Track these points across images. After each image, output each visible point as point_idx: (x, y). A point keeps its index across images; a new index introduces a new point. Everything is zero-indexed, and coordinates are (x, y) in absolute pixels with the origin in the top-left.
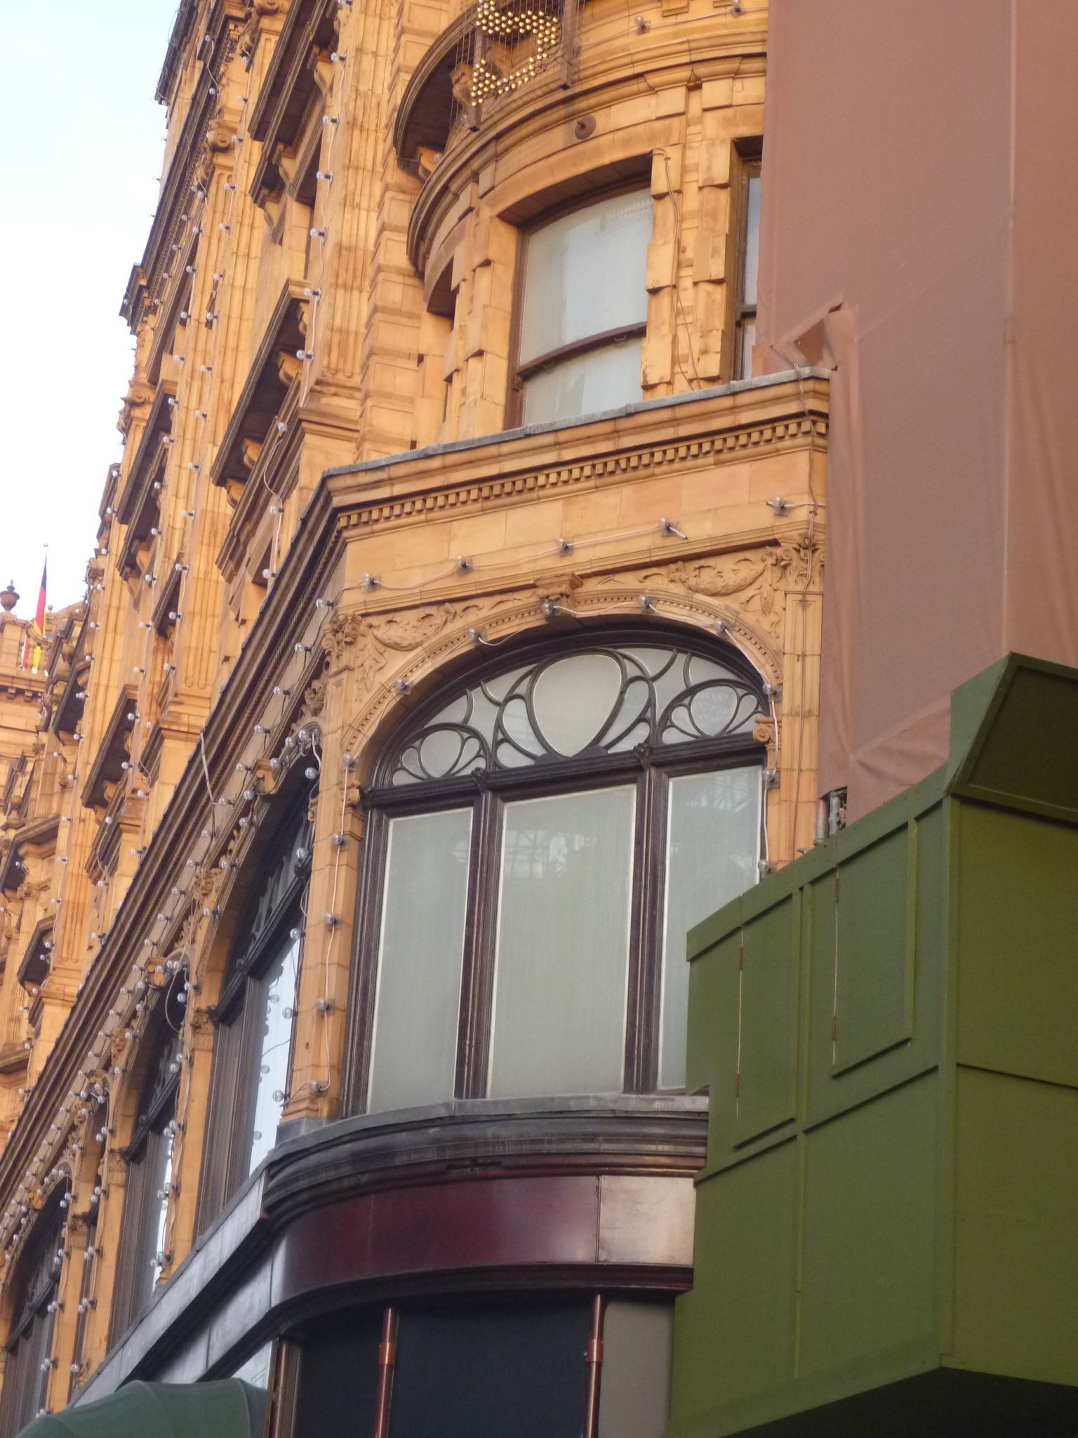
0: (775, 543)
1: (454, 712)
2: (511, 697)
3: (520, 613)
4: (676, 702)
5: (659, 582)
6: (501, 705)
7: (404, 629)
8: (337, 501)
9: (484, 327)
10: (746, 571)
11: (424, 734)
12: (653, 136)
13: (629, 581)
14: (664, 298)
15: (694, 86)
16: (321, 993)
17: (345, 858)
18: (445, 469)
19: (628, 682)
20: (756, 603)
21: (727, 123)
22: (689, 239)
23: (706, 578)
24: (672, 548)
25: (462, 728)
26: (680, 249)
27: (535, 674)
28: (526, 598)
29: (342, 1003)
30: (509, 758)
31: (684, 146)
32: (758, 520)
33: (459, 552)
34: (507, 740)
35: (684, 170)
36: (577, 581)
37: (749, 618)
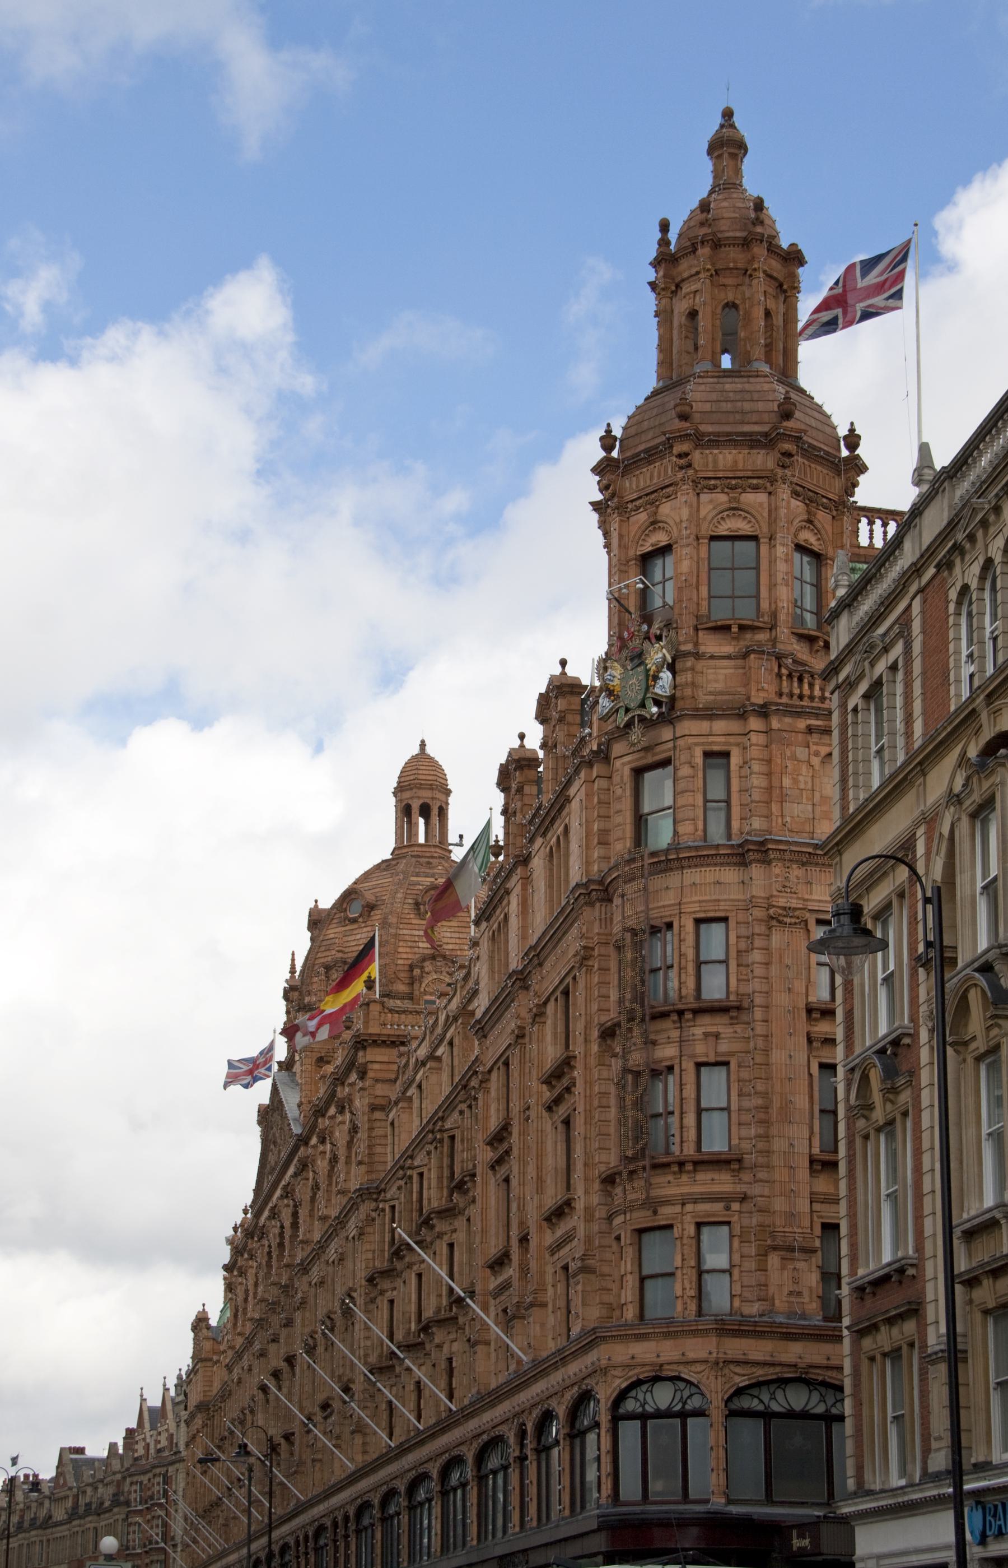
1: (633, 1393)
4: (688, 1397)
5: (681, 1368)
7: (617, 1372)
10: (702, 1368)
12: (673, 1219)
13: (675, 1367)
15: (683, 1204)
17: (609, 1434)
19: (676, 1391)
21: (693, 1217)
23: (693, 1368)
24: (684, 1359)
25: (636, 1398)
26: (683, 1255)
27: (653, 1385)
30: (648, 1408)
32: (703, 1355)
36: (661, 1365)
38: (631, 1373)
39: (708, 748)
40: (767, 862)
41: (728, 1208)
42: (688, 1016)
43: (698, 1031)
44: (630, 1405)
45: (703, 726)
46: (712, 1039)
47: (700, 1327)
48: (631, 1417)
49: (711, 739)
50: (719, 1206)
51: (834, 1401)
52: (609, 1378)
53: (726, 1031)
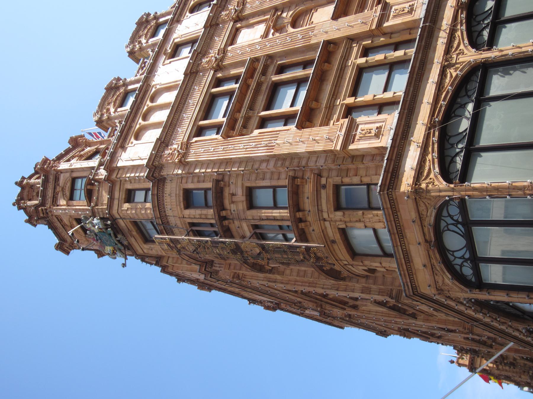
0: (416, 199)
1: (458, 268)
2: (453, 255)
3: (434, 254)
4: (452, 219)
5: (426, 224)
6: (455, 257)
8: (412, 294)
9: (375, 262)
10: (422, 204)
11: (463, 275)
13: (426, 230)
14: (367, 224)
15: (325, 220)
16: (525, 298)
17: (493, 293)
18: (403, 270)
19: (449, 230)
20: (429, 202)
22: (354, 219)
25: (461, 266)
26: (357, 221)
27: (448, 250)
28: (431, 253)
29: (527, 293)
30: (467, 256)
31: (336, 221)
33: (422, 268)
34: (463, 256)
35: (341, 221)
36: (426, 241)
37: (433, 204)
38: (438, 268)
39: (123, 201)
40: (161, 167)
41: (324, 187)
42: (224, 213)
43: (233, 207)
44: (467, 271)
45: (116, 202)
46: (235, 199)
47: (389, 206)
48: (477, 272)
49: (120, 199)
50: (323, 192)
51: (466, 97)
52: (446, 288)
53: (233, 189)
